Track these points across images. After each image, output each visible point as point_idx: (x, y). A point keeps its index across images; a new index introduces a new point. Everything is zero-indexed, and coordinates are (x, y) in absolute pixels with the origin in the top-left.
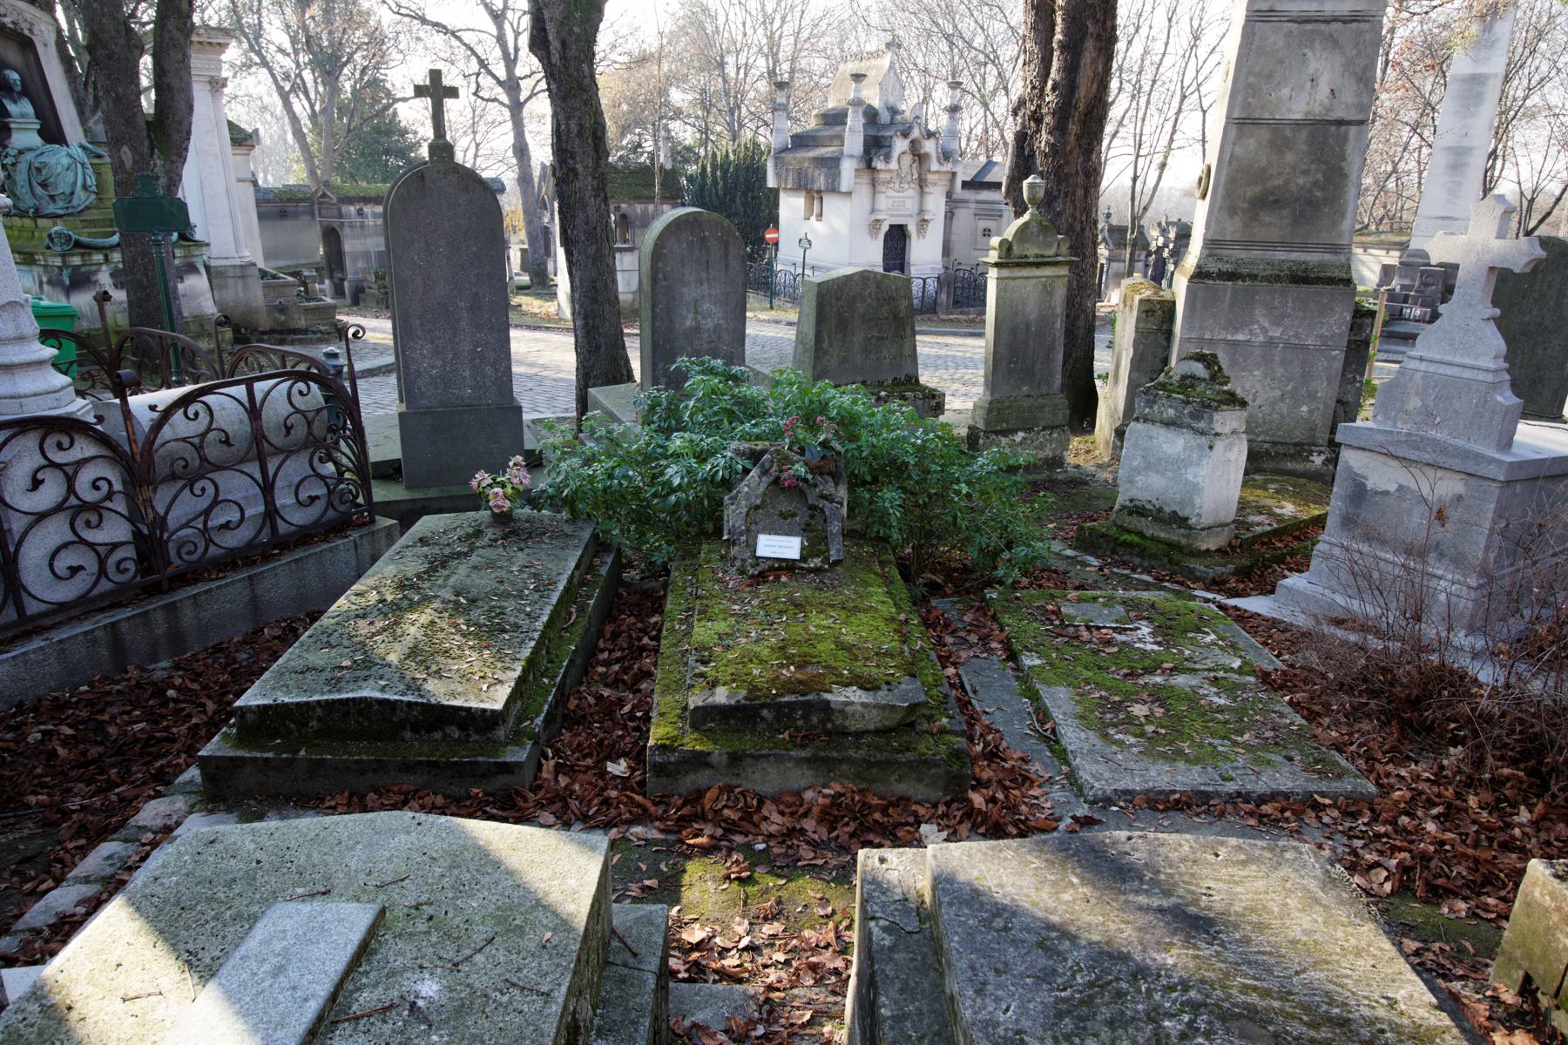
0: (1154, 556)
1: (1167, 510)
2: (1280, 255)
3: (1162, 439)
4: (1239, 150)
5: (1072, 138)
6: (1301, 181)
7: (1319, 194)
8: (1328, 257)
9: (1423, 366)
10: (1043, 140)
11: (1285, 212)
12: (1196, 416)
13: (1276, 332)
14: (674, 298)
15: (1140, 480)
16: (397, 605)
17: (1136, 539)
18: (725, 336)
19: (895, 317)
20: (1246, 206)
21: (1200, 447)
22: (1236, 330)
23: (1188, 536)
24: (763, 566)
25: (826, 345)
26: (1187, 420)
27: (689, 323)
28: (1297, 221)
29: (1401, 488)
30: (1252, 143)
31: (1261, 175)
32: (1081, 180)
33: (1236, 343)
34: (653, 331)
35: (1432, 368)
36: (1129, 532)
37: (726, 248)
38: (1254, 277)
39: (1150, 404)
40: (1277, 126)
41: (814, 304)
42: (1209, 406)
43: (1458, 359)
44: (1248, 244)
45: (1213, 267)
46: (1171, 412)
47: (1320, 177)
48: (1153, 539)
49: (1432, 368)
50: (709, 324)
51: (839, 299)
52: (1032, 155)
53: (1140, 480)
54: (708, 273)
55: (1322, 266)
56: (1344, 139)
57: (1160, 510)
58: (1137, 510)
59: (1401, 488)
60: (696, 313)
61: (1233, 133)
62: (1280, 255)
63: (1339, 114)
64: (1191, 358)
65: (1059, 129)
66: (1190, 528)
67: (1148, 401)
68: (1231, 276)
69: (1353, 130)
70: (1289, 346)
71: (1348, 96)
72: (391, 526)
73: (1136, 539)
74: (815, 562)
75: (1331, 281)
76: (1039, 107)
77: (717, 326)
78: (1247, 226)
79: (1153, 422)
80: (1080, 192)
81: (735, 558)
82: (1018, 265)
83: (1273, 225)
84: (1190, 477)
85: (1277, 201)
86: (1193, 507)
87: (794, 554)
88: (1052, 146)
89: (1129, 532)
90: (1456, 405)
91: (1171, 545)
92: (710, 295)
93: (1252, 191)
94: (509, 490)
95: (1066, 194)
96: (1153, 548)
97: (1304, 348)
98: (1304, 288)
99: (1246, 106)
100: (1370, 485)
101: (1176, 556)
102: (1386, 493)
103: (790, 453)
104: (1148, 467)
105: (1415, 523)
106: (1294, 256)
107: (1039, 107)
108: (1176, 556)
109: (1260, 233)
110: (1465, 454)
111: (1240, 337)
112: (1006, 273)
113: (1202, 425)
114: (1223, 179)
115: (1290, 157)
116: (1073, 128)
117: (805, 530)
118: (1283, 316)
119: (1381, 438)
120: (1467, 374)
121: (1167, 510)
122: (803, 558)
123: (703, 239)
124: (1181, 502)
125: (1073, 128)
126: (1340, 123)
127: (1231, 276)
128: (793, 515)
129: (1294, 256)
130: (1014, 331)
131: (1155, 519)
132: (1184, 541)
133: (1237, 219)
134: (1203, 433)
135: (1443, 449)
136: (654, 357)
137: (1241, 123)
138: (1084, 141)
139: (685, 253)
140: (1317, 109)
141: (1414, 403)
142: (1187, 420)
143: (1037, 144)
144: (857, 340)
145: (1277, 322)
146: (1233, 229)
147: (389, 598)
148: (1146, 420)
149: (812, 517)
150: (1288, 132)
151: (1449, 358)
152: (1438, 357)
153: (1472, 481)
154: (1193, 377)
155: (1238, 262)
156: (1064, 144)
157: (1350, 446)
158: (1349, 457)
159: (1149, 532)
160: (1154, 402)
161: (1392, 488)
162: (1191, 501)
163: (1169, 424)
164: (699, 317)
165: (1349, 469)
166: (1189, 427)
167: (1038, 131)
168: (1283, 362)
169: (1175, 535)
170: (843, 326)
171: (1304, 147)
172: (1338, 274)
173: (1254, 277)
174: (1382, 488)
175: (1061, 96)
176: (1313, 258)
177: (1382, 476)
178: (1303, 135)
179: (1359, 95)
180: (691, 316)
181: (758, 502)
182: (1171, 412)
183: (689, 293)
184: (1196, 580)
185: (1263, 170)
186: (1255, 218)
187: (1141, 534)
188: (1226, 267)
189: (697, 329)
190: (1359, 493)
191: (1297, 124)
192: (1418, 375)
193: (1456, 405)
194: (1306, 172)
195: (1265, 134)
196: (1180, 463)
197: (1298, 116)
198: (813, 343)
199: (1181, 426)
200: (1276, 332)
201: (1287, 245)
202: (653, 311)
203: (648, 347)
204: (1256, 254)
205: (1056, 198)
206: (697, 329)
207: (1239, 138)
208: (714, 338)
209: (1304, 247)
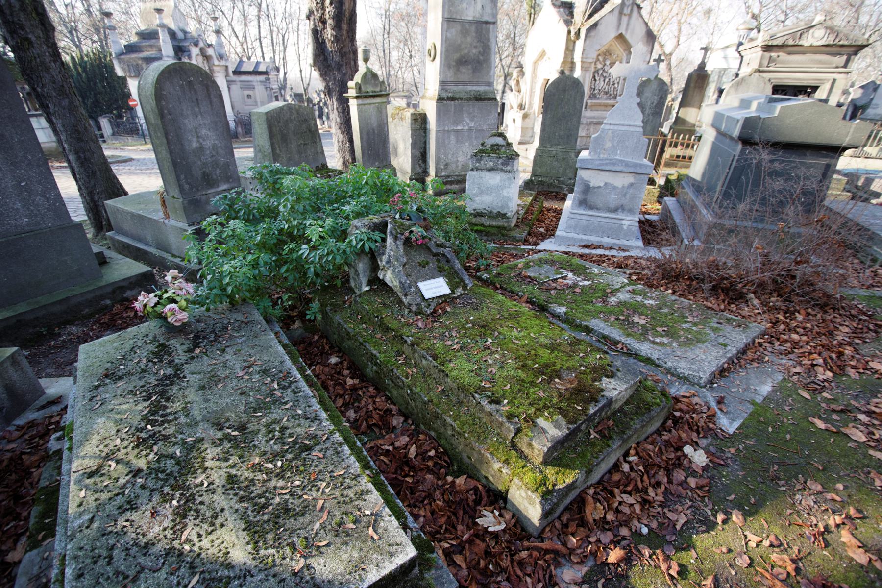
0: (493, 234)
1: (495, 211)
2: (470, 88)
3: (487, 178)
4: (449, 35)
5: (345, 32)
6: (474, 51)
7: (481, 58)
8: (487, 88)
9: (612, 127)
10: (329, 33)
11: (470, 67)
12: (505, 164)
13: (472, 124)
14: (180, 128)
15: (478, 199)
16: (158, 471)
17: (482, 228)
18: (221, 151)
19: (310, 131)
20: (454, 64)
21: (509, 179)
22: (457, 125)
23: (508, 222)
24: (433, 305)
25: (278, 151)
26: (500, 166)
27: (194, 145)
28: (475, 70)
29: (606, 184)
30: (453, 31)
31: (458, 48)
32: (352, 56)
33: (457, 131)
34: (171, 153)
35: (616, 128)
36: (476, 225)
37: (208, 90)
38: (461, 99)
39: (479, 161)
40: (463, 23)
41: (265, 126)
42: (511, 158)
43: (626, 123)
44: (457, 83)
45: (445, 95)
46: (491, 164)
47: (481, 49)
48: (489, 226)
49: (616, 128)
50: (208, 144)
51: (279, 122)
52: (324, 42)
53: (478, 199)
54: (200, 108)
55: (485, 92)
56: (488, 31)
57: (491, 212)
58: (479, 214)
59: (606, 184)
60: (198, 137)
61: (446, 26)
62: (470, 88)
63: (485, 18)
64: (495, 135)
65: (337, 27)
66: (508, 218)
67: (477, 160)
68: (452, 99)
69: (491, 26)
70: (478, 131)
71: (488, 10)
72: (13, 355)
73: (482, 228)
74: (459, 291)
75: (489, 99)
76: (323, 14)
77: (214, 145)
78: (455, 74)
79: (482, 170)
80: (352, 62)
81: (410, 305)
82: (366, 97)
83: (466, 73)
84: (505, 194)
85: (466, 61)
86: (508, 208)
87: (446, 290)
88: (335, 37)
89: (476, 225)
90: (627, 143)
91: (499, 227)
92: (204, 124)
93: (456, 56)
94: (184, 303)
95: (347, 64)
96: (493, 231)
97: (482, 130)
98: (480, 103)
99: (450, 12)
100: (592, 185)
101: (505, 232)
102: (599, 187)
103: (402, 221)
104: (482, 192)
105: (613, 199)
106: (475, 88)
107: (323, 14)
108: (505, 232)
109: (462, 77)
110: (636, 165)
111: (459, 128)
112: (360, 101)
113: (509, 168)
114: (444, 50)
115: (469, 39)
116: (344, 26)
117: (440, 272)
118: (474, 117)
119: (598, 162)
120: (632, 129)
121: (495, 211)
122: (453, 292)
123: (190, 84)
124: (502, 206)
125: (344, 26)
126: (487, 23)
127: (452, 99)
128: (427, 263)
129: (475, 88)
130: (368, 134)
131: (489, 217)
132: (506, 225)
133: (451, 71)
134: (509, 172)
135: (627, 164)
136: (176, 171)
137: (449, 21)
138: (350, 34)
139: (180, 93)
140: (478, 15)
141: (608, 144)
142: (500, 166)
143: (325, 36)
144: (293, 146)
145: (472, 120)
146: (450, 76)
147: (142, 463)
148: (477, 169)
149: (438, 261)
150: (467, 26)
151: (622, 122)
152: (618, 122)
153: (637, 176)
154: (497, 145)
155: (454, 92)
156: (342, 36)
157: (582, 168)
158: (581, 173)
159: (487, 224)
160: (481, 160)
161: (602, 184)
162: (507, 205)
163: (490, 170)
164: (201, 140)
165: (582, 179)
166: (502, 170)
167: (325, 28)
168: (476, 138)
169: (501, 223)
170: (285, 139)
171: (474, 34)
172: (491, 96)
173: (461, 99)
174: (597, 185)
175: (335, 8)
176: (482, 89)
177: (595, 179)
178: (473, 28)
179: (492, 9)
180: (195, 139)
181: (405, 260)
182: (491, 164)
183: (189, 123)
184: (518, 241)
185: (459, 45)
186: (458, 70)
187: (483, 225)
188: (450, 95)
189: (201, 148)
190: (587, 189)
191: (470, 22)
192: (610, 132)
193: (627, 143)
194: (476, 47)
195: (458, 27)
196: (499, 188)
197: (471, 18)
198: (270, 151)
199: (497, 170)
200: (472, 124)
201: (471, 83)
202: (167, 138)
203: (168, 164)
204: (460, 87)
205: (342, 65)
206: (201, 148)
207: (448, 28)
208: (214, 153)
209: (478, 84)
